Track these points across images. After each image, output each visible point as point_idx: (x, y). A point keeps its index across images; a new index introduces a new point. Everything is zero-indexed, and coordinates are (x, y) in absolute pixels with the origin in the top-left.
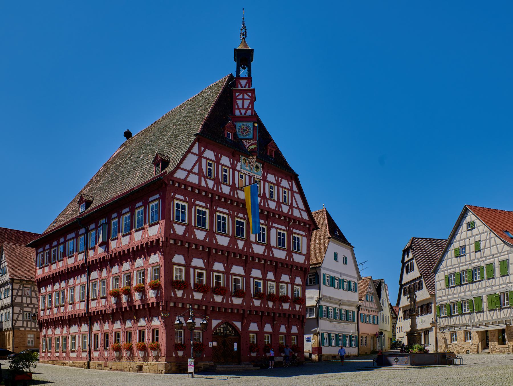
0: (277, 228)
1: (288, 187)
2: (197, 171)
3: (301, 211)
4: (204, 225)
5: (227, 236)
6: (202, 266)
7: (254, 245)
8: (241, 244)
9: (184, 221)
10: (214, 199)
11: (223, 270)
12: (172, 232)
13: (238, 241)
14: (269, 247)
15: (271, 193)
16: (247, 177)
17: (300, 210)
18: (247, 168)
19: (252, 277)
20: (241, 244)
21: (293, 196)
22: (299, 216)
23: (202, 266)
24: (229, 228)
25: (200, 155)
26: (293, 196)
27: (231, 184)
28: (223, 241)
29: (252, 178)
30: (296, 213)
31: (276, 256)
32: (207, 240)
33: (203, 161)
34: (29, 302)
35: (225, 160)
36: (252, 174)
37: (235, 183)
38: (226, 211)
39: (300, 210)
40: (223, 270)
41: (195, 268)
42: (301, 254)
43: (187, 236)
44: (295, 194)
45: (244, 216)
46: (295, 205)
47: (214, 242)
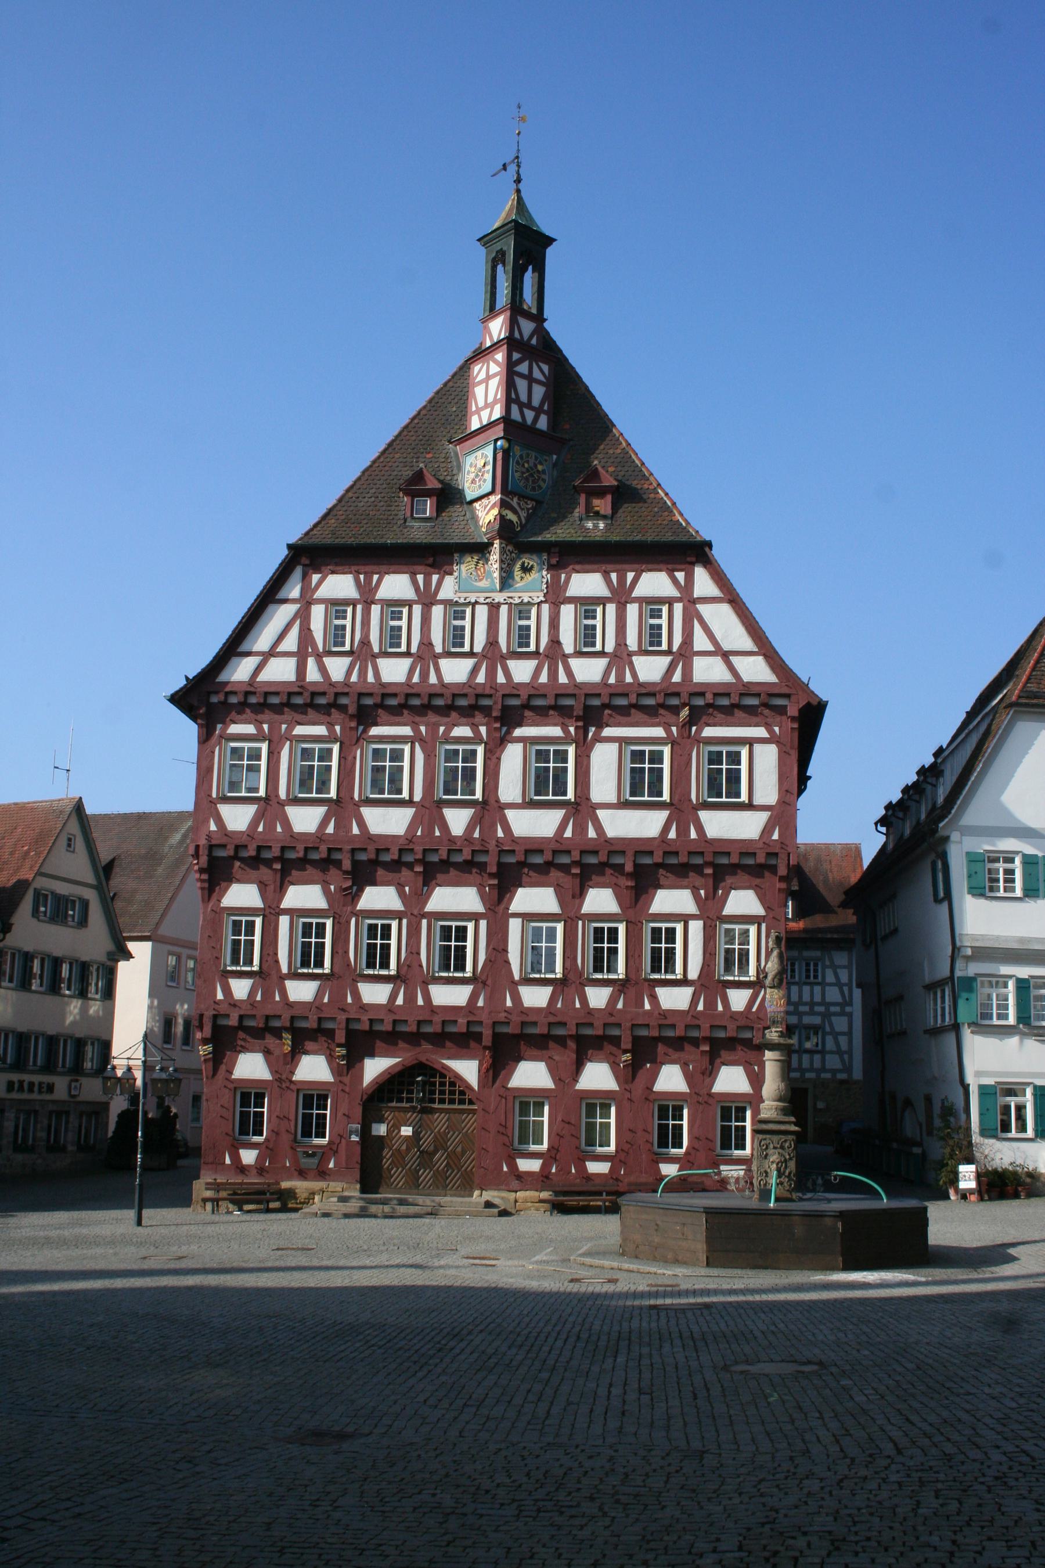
0: (622, 741)
1: (676, 593)
2: (294, 648)
3: (735, 660)
4: (323, 786)
5: (409, 803)
6: (322, 903)
7: (510, 814)
8: (458, 820)
9: (257, 790)
10: (361, 709)
11: (397, 905)
12: (213, 827)
13: (449, 814)
14: (582, 809)
15: (588, 635)
16: (482, 612)
17: (726, 656)
18: (484, 584)
19: (516, 915)
20: (458, 820)
21: (691, 616)
22: (727, 677)
23: (322, 903)
24: (414, 781)
25: (307, 602)
26: (691, 616)
27: (414, 649)
28: (388, 822)
29: (504, 610)
30: (708, 671)
31: (611, 833)
32: (330, 829)
33: (318, 612)
34: (818, 998)
35: (396, 585)
36: (499, 597)
37: (431, 644)
38: (406, 731)
39: (726, 656)
40: (397, 905)
41: (294, 913)
42: (750, 806)
43: (260, 829)
44: (703, 609)
45: (477, 732)
46: (700, 642)
47: (356, 830)
